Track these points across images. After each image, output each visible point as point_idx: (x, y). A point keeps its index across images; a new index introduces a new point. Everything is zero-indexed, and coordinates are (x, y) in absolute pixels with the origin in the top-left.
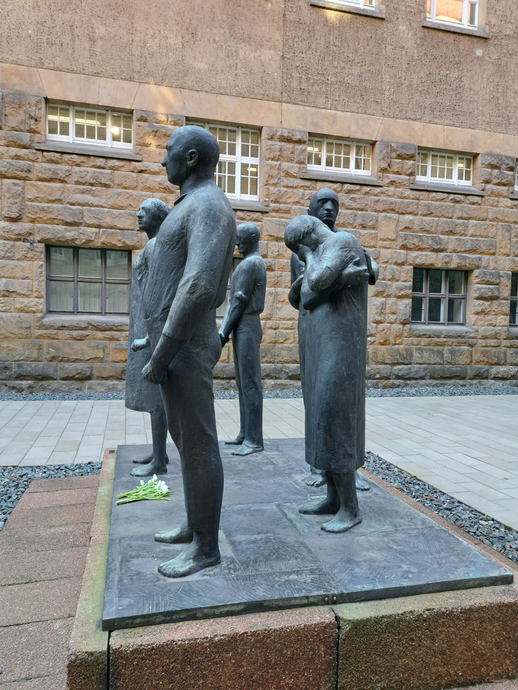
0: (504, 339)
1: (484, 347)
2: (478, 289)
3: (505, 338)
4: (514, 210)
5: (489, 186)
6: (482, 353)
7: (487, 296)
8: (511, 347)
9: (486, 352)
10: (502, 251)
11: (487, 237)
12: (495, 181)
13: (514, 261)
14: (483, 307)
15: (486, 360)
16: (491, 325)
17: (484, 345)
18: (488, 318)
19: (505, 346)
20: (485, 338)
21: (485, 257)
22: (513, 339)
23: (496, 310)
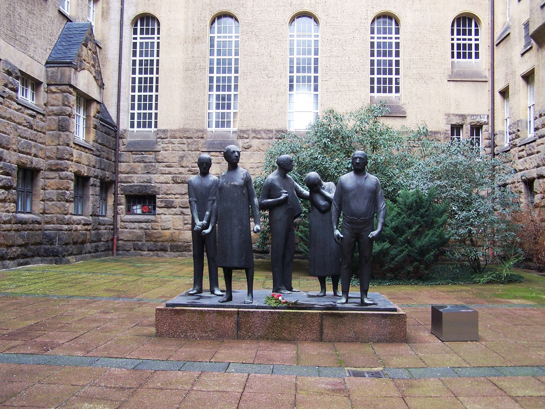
0: (14, 224)
1: (4, 231)
2: (3, 179)
3: (14, 222)
4: (19, 113)
5: (7, 90)
6: (3, 237)
7: (7, 185)
8: (17, 230)
9: (6, 234)
10: (13, 146)
11: (5, 133)
12: (10, 86)
13: (19, 156)
14: (5, 195)
15: (6, 243)
16: (8, 211)
17: (5, 229)
18: (7, 204)
19: (15, 230)
20: (5, 223)
21: (5, 151)
22: (19, 223)
23: (11, 198)
